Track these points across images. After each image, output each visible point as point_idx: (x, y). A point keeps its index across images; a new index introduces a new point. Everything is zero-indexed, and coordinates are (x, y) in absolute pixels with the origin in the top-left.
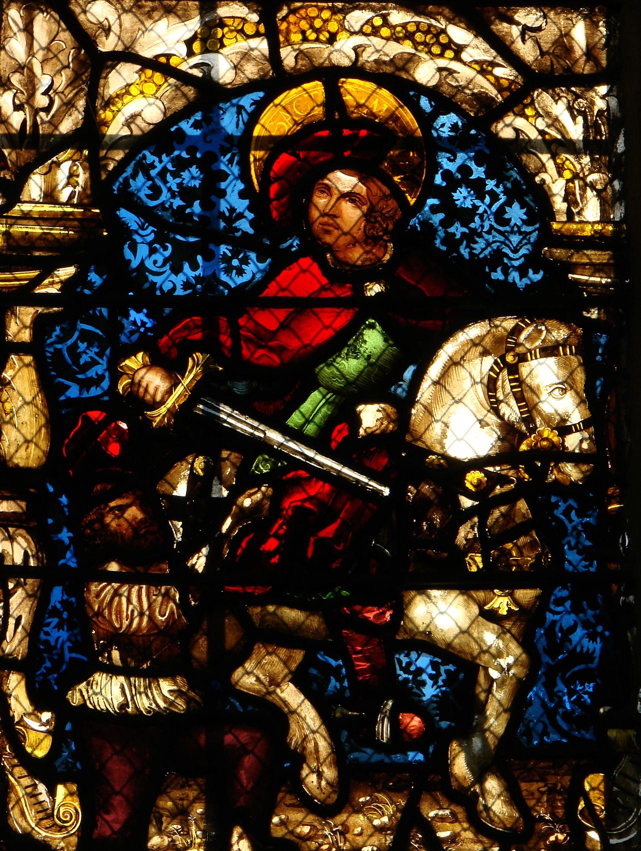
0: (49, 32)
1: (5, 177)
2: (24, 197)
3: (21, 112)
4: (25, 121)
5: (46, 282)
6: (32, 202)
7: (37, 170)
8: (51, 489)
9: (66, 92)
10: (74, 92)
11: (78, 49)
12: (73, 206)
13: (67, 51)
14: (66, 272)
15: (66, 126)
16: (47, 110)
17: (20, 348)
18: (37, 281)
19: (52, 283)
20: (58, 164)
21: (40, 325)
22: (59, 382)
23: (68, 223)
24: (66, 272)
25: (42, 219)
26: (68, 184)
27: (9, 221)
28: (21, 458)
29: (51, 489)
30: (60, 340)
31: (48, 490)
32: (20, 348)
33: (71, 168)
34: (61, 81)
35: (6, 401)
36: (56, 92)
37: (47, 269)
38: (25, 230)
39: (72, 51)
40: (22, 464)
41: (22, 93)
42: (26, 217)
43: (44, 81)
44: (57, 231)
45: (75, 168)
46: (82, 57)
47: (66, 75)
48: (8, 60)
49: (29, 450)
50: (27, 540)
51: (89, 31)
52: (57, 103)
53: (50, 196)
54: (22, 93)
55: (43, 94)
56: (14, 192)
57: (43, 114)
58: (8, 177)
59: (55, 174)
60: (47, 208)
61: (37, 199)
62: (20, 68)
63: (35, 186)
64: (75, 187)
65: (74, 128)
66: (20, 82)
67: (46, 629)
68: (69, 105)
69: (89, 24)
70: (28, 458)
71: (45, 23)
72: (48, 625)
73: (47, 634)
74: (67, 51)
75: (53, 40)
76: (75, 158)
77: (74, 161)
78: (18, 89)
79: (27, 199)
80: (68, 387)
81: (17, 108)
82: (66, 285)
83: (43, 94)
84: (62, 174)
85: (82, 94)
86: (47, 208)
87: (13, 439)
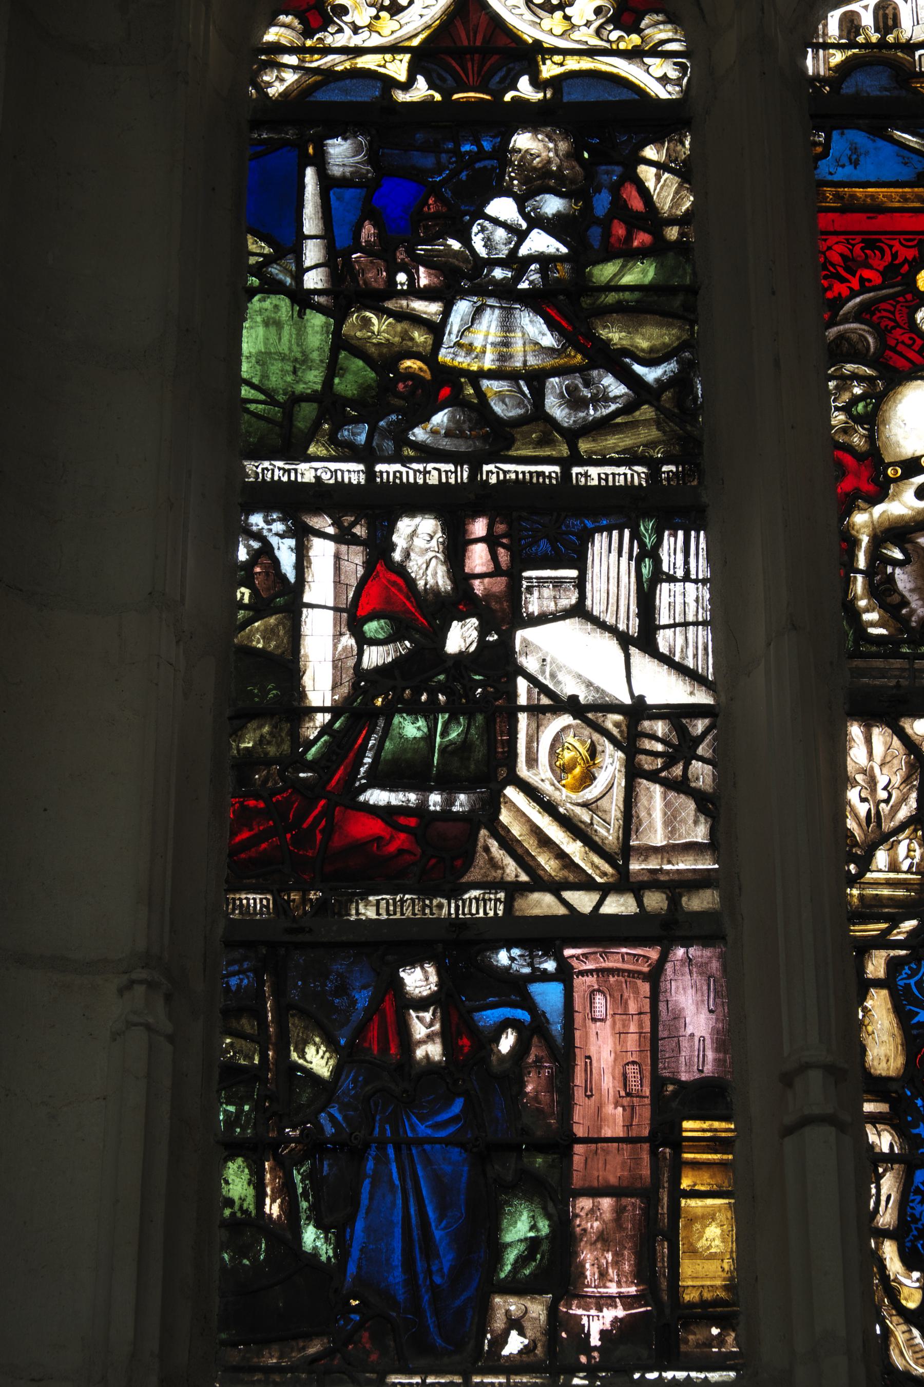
0: (885, 743)
1: (856, 853)
2: (873, 867)
3: (866, 803)
4: (869, 810)
5: (895, 932)
6: (880, 871)
7: (881, 847)
8: (909, 1093)
9: (901, 788)
10: (908, 787)
11: (908, 755)
12: (912, 873)
13: (900, 757)
14: (909, 925)
15: (903, 813)
16: (887, 801)
17: (878, 983)
18: (888, 931)
19: (899, 933)
20: (899, 842)
21: (893, 965)
22: (910, 1009)
23: (910, 887)
24: (909, 925)
25: (889, 883)
26: (907, 857)
27: (862, 886)
28: (883, 1070)
29: (909, 1093)
30: (909, 977)
31: (906, 1094)
32: (878, 983)
33: (908, 845)
34: (897, 780)
35: (868, 1024)
36: (893, 788)
37: (895, 922)
38: (875, 892)
39: (904, 757)
40: (884, 1074)
41: (866, 789)
42: (876, 884)
43: (882, 781)
44: (900, 893)
45: (912, 845)
46: (912, 761)
47: (901, 775)
48: (853, 764)
49: (889, 1063)
50: (891, 1134)
51: (917, 742)
52: (895, 794)
53: (894, 867)
54: (866, 789)
55: (883, 789)
56: (865, 863)
57: (883, 805)
58: (859, 852)
59: (897, 849)
60: (892, 875)
61: (884, 869)
62: (863, 771)
63: (881, 858)
64: (913, 859)
65: (909, 814)
66: (864, 781)
67: (911, 1204)
68: (904, 799)
69: (916, 737)
70: (888, 1069)
71: (881, 737)
72: (913, 1201)
73: (912, 1208)
74: (900, 757)
75: (889, 749)
76: (911, 837)
77: (911, 840)
78: (862, 787)
79: (875, 869)
80: (918, 1013)
81: (863, 800)
82: (911, 933)
83: (883, 789)
84: (902, 849)
85: (914, 789)
86: (892, 875)
87: (875, 1054)
